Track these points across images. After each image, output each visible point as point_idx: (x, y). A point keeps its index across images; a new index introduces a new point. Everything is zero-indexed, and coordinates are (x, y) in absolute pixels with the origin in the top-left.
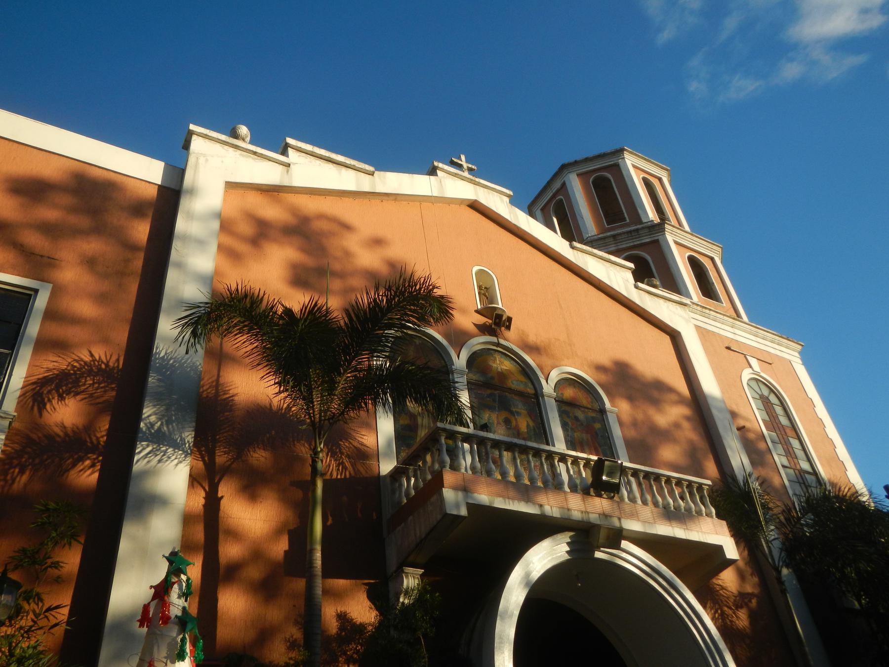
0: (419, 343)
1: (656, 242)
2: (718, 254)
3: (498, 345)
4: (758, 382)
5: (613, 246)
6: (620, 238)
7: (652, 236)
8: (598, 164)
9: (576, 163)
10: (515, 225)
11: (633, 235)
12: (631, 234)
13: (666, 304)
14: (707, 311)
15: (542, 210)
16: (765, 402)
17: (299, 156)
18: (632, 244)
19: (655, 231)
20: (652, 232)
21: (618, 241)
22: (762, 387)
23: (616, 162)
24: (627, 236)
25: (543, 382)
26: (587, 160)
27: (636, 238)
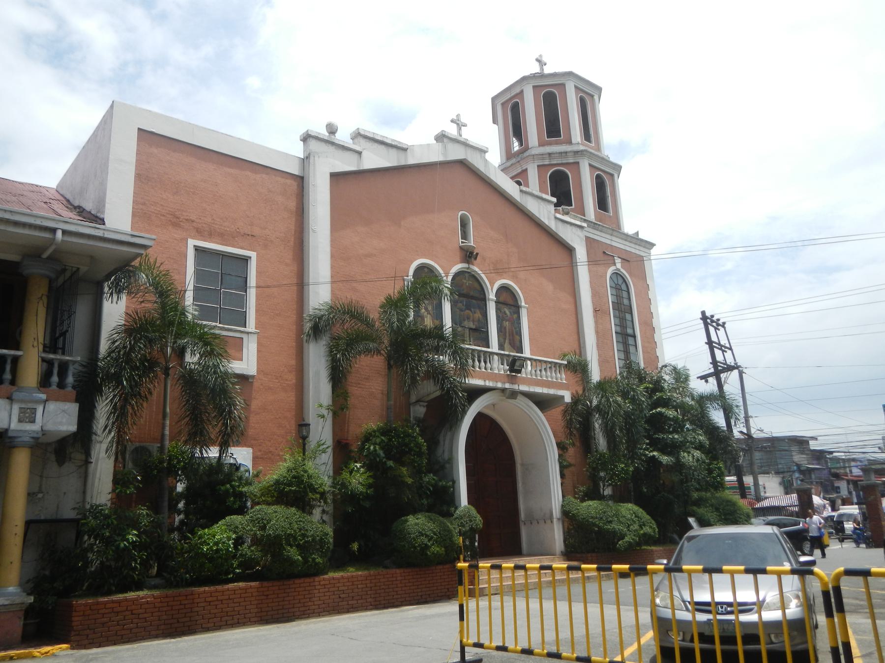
1: (578, 163)
4: (618, 276)
10: (488, 177)
15: (503, 104)
16: (617, 288)
18: (560, 162)
22: (620, 278)
25: (490, 291)
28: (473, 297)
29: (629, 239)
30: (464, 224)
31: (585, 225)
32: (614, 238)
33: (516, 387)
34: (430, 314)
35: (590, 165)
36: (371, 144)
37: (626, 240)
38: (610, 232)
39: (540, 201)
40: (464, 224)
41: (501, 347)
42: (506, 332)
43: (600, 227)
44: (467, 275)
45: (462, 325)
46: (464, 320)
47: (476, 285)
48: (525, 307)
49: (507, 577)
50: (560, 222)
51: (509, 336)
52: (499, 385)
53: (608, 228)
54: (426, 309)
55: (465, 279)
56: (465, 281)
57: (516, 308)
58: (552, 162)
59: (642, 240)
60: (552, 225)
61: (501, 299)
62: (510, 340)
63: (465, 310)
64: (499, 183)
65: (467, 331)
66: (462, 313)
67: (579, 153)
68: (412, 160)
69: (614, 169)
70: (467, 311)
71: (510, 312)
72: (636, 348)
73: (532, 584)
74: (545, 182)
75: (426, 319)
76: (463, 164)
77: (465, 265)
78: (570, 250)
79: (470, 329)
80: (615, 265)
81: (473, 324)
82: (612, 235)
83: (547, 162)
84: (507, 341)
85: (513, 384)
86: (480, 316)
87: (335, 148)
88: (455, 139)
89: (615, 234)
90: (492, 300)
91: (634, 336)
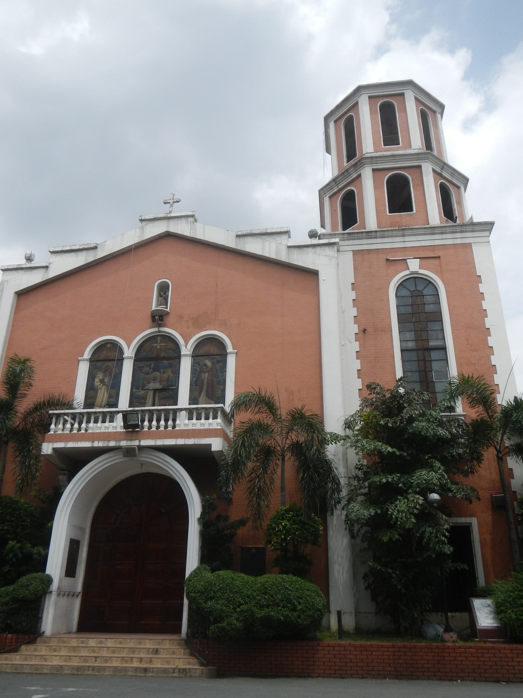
0: (110, 346)
1: (359, 176)
2: (426, 160)
3: (160, 332)
5: (336, 187)
6: (338, 180)
7: (358, 171)
8: (346, 106)
9: (332, 113)
11: (345, 175)
12: (344, 175)
13: (314, 249)
14: (373, 234)
17: (57, 255)
19: (358, 166)
20: (356, 169)
21: (338, 183)
23: (357, 100)
24: (342, 177)
26: (338, 107)
27: (348, 177)
28: (164, 358)
29: (438, 231)
30: (163, 289)
31: (337, 240)
32: (407, 239)
33: (136, 443)
34: (105, 385)
35: (374, 170)
36: (61, 256)
37: (433, 234)
38: (400, 233)
39: (265, 237)
40: (163, 289)
41: (193, 400)
42: (202, 386)
43: (379, 234)
44: (159, 339)
45: (146, 388)
46: (149, 383)
47: (171, 345)
48: (231, 353)
49: (36, 656)
50: (296, 249)
51: (207, 387)
52: (112, 444)
53: (392, 230)
54: (102, 381)
55: (156, 342)
56: (156, 345)
57: (223, 355)
58: (340, 187)
59: (480, 224)
60: (283, 257)
61: (202, 352)
62: (207, 391)
63: (153, 372)
64: (206, 239)
65: (151, 394)
66: (148, 376)
67: (359, 164)
68: (100, 254)
69: (418, 159)
70: (155, 373)
71: (213, 363)
72: (448, 363)
73: (49, 667)
74: (336, 210)
75: (99, 391)
76: (168, 235)
77: (155, 329)
78: (314, 274)
79: (155, 390)
80: (409, 269)
81: (160, 385)
82: (404, 236)
83: (335, 190)
84: (203, 395)
85: (131, 440)
86: (171, 374)
87: (24, 272)
88: (154, 218)
89: (406, 232)
90: (186, 355)
91: (444, 348)
